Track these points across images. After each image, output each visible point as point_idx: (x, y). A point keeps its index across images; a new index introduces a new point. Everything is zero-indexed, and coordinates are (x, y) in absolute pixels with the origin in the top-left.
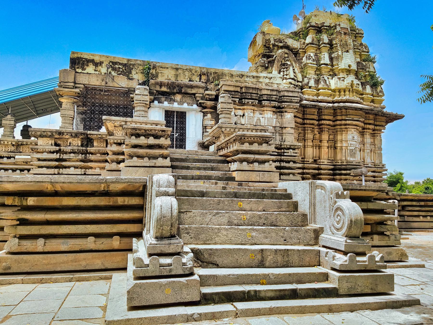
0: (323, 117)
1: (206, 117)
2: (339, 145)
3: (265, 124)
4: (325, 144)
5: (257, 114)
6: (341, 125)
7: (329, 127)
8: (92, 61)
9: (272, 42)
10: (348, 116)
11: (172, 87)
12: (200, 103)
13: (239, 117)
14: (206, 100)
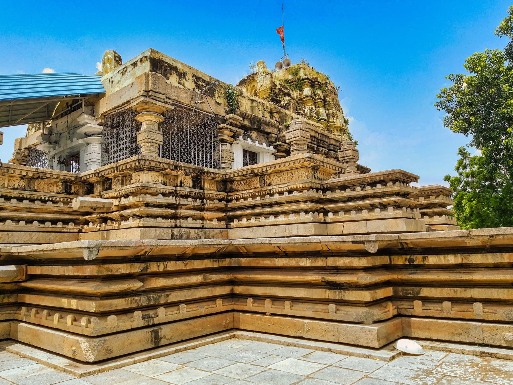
8: (175, 69)
9: (278, 87)
12: (277, 145)
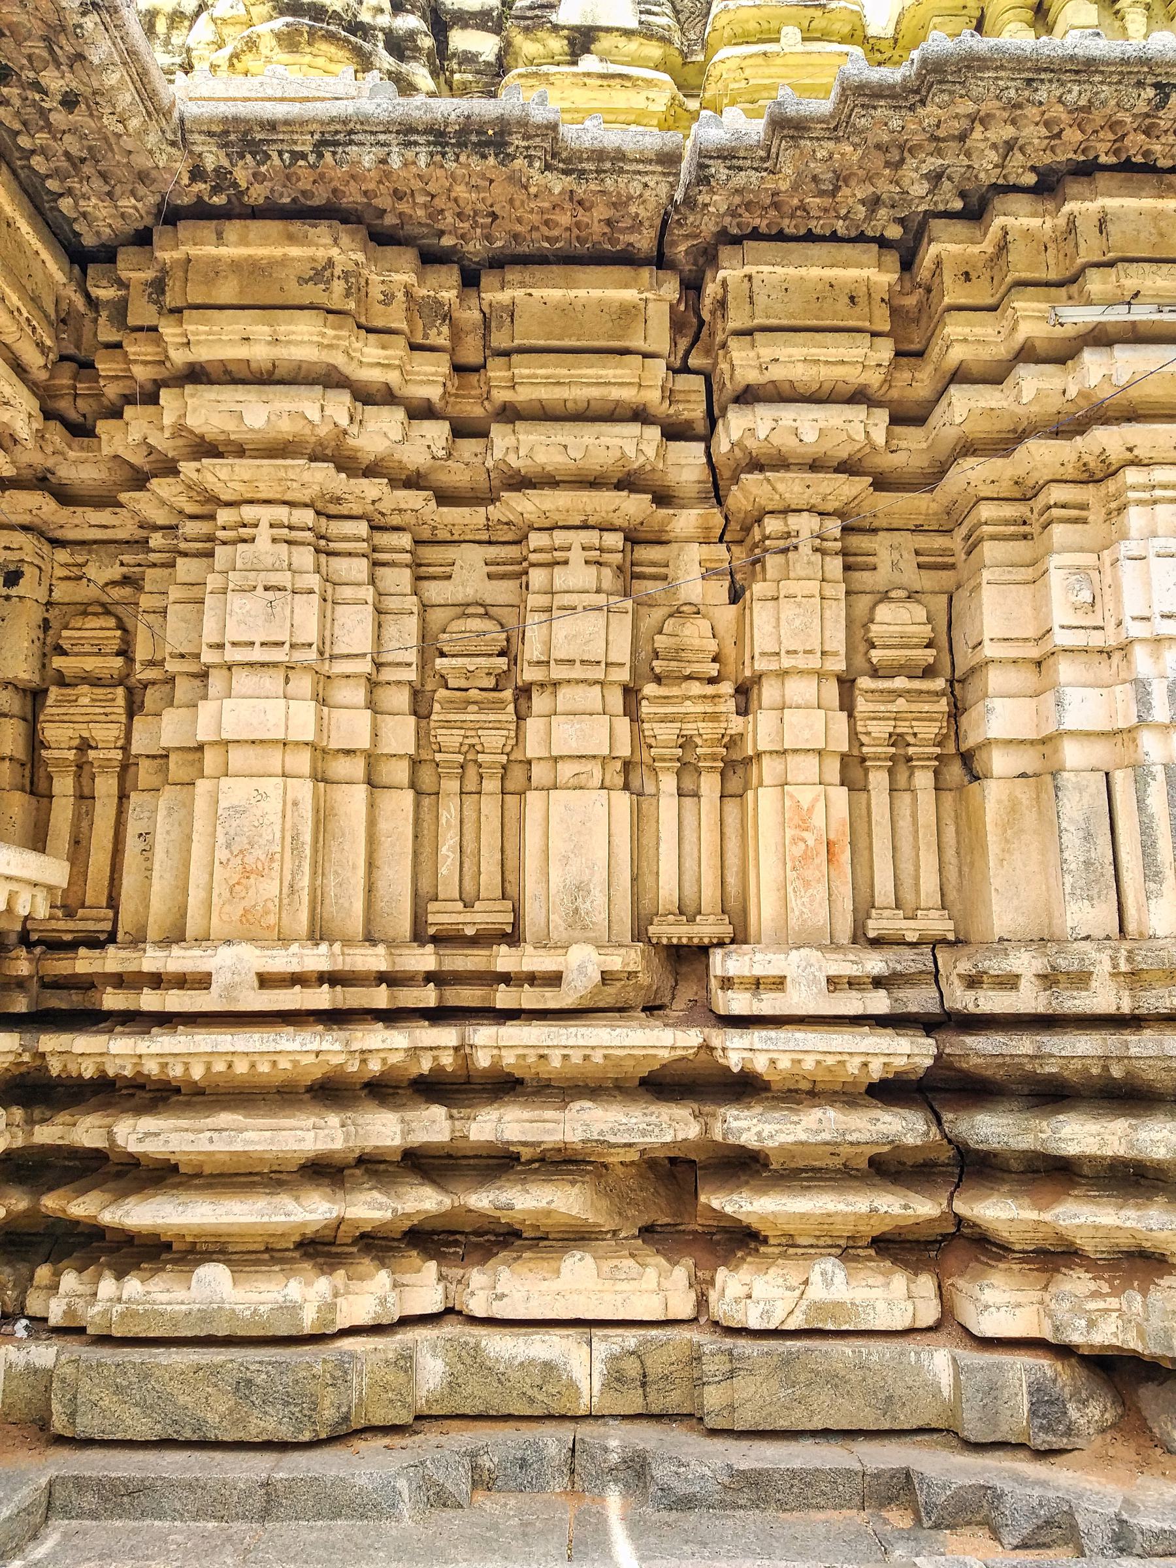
0: (744, 363)
2: (1001, 716)
4: (798, 721)
6: (1005, 443)
7: (846, 488)
10: (1096, 283)
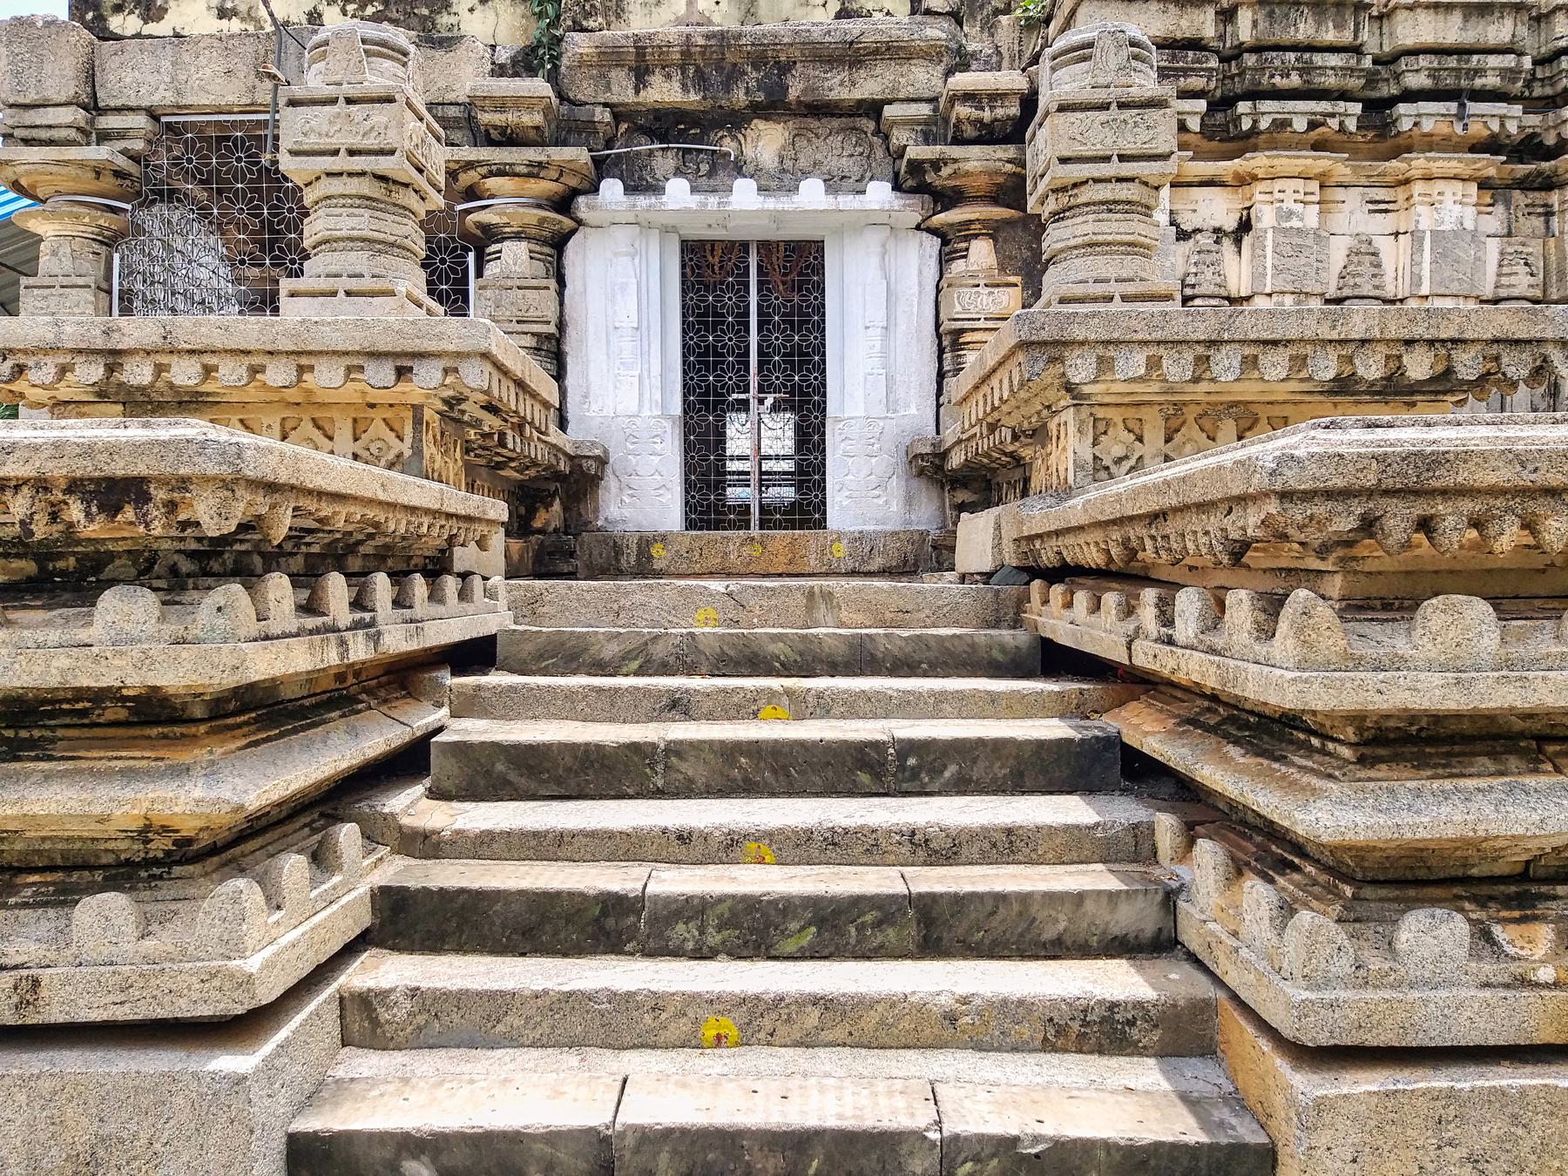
1: (958, 266)
3: (1417, 280)
5: (1353, 216)
11: (720, 69)
12: (916, 167)
13: (1205, 240)
14: (958, 141)
